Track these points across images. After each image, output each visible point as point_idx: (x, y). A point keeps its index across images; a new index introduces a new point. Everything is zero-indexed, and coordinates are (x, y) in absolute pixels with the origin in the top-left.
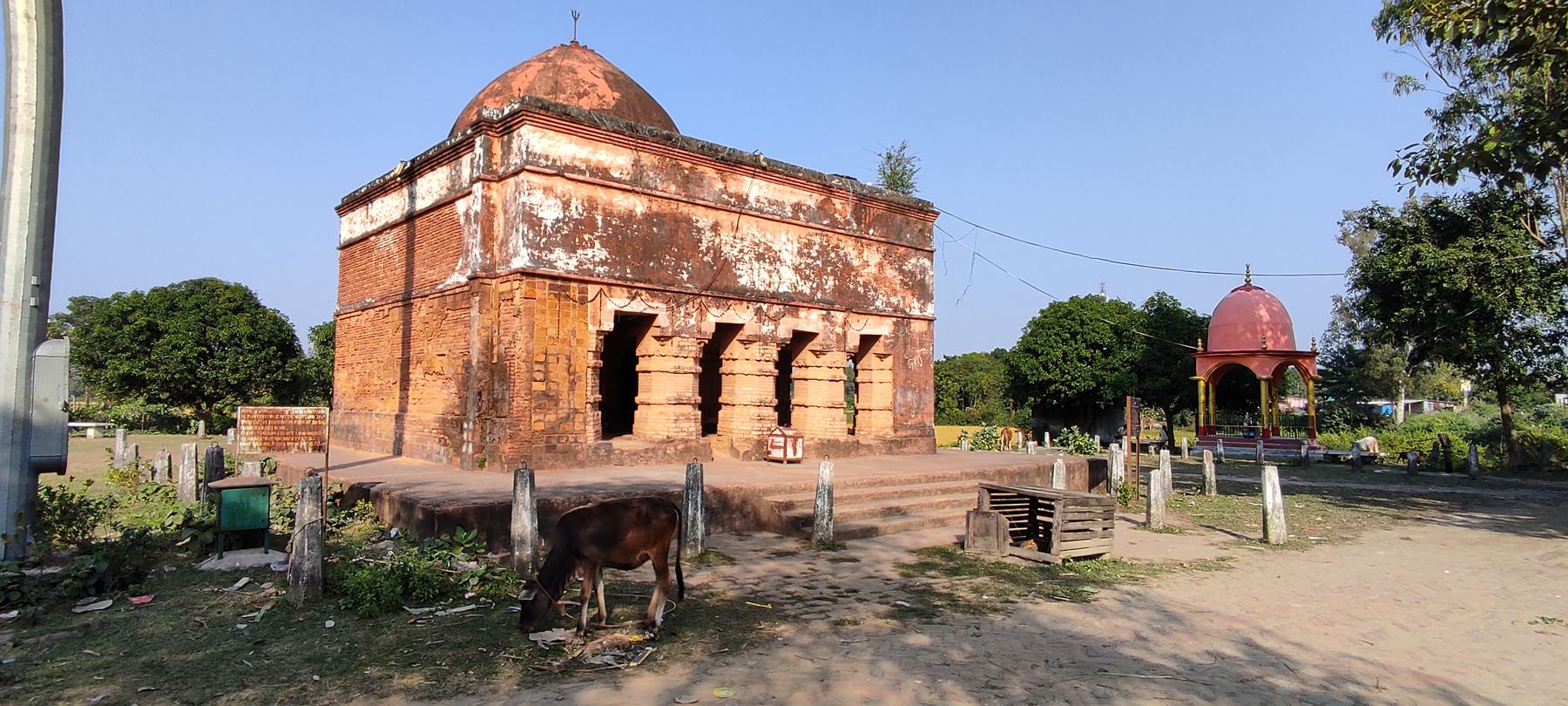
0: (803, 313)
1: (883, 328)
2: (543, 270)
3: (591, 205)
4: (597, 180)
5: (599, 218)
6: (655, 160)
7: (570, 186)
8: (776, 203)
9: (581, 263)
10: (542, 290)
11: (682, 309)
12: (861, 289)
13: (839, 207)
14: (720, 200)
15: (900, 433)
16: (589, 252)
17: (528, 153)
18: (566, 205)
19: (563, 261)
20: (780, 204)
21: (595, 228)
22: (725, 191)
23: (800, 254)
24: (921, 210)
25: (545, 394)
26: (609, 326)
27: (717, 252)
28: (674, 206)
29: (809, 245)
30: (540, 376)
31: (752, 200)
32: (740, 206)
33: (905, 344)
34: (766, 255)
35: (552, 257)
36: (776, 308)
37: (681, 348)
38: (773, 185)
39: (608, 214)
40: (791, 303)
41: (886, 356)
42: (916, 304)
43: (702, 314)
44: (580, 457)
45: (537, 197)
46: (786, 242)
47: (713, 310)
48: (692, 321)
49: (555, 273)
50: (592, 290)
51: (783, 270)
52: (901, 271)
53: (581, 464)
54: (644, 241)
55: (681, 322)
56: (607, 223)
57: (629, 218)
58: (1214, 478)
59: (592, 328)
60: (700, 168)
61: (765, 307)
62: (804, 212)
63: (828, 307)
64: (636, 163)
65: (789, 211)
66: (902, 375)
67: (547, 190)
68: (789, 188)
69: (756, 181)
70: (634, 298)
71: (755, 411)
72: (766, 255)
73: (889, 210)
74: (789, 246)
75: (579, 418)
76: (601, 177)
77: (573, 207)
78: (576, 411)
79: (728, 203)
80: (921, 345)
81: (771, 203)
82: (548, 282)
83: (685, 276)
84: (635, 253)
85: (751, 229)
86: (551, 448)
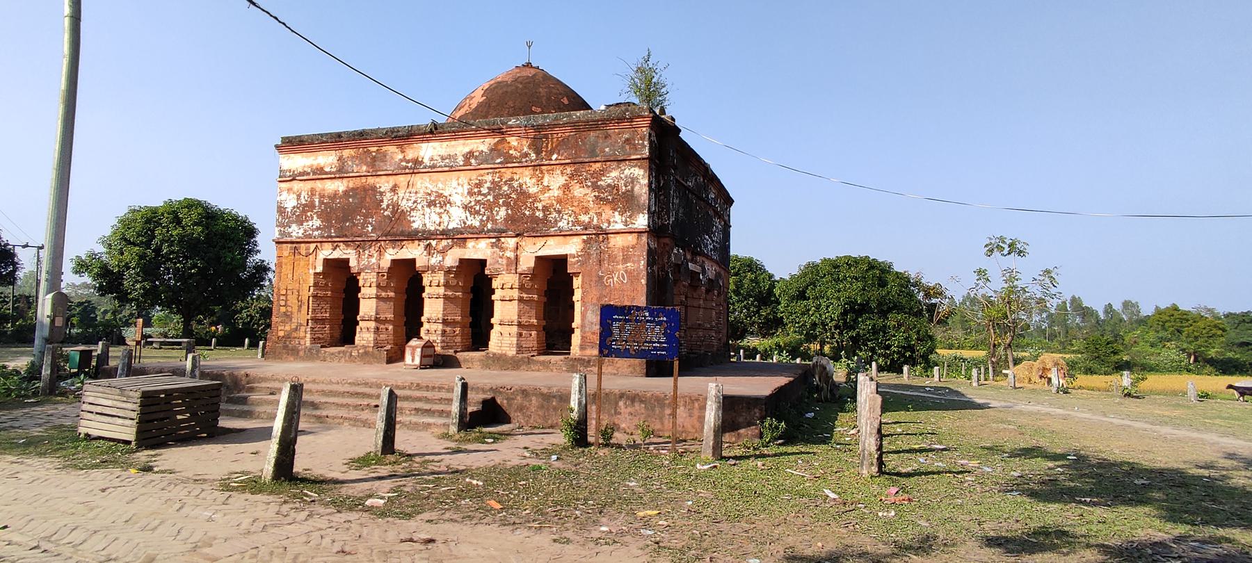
0: (470, 244)
1: (570, 248)
3: (313, 192)
6: (352, 152)
7: (302, 184)
12: (540, 214)
18: (299, 196)
19: (296, 231)
21: (314, 207)
22: (404, 160)
23: (470, 193)
24: (621, 119)
26: (320, 269)
27: (395, 207)
28: (364, 180)
29: (479, 185)
30: (283, 303)
31: (427, 161)
32: (416, 167)
33: (600, 262)
36: (444, 243)
39: (322, 196)
40: (458, 237)
43: (380, 252)
44: (301, 353)
45: (285, 195)
46: (457, 188)
47: (391, 251)
48: (374, 260)
50: (313, 246)
52: (595, 187)
55: (364, 262)
56: (321, 203)
57: (334, 196)
59: (312, 271)
60: (384, 148)
61: (434, 243)
62: (476, 158)
63: (498, 235)
65: (460, 161)
67: (289, 190)
68: (461, 141)
69: (431, 144)
70: (334, 249)
72: (438, 201)
73: (578, 130)
74: (460, 190)
75: (303, 329)
78: (301, 325)
81: (443, 159)
83: (370, 229)
84: (338, 220)
85: (423, 184)
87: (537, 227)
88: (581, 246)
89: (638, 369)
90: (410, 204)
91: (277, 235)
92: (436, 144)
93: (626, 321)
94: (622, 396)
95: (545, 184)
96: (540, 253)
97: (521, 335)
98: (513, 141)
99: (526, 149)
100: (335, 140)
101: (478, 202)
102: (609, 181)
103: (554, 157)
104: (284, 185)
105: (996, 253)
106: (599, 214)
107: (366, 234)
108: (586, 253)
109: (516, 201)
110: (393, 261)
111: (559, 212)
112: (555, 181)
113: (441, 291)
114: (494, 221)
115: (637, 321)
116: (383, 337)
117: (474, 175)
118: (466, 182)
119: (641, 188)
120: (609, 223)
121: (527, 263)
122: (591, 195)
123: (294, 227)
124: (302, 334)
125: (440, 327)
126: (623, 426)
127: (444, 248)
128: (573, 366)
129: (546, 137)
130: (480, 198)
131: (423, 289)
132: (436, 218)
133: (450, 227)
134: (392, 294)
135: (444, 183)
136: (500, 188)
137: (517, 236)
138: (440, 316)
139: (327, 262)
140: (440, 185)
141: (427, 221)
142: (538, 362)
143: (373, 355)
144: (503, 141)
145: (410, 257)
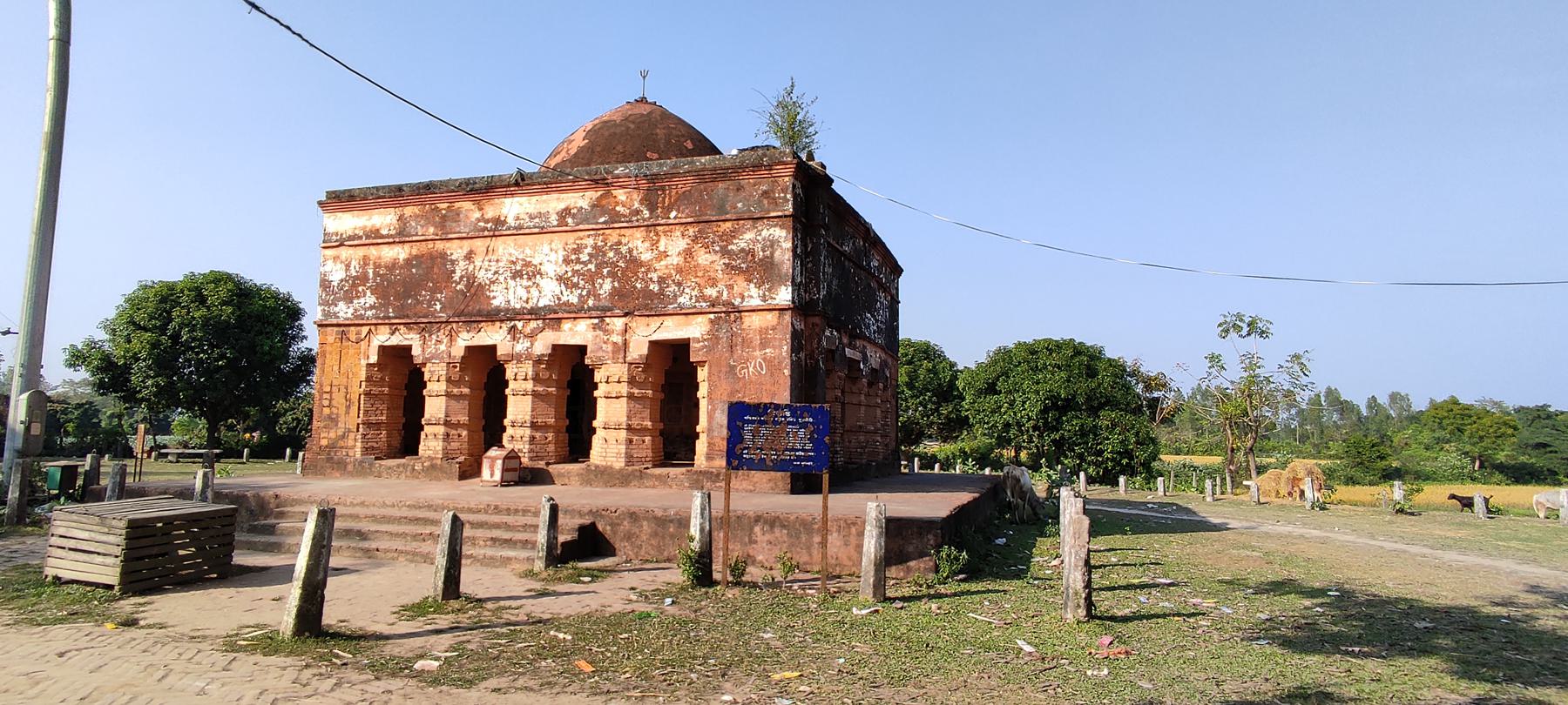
0: (566, 325)
1: (693, 329)
3: (365, 261)
6: (416, 210)
7: (351, 251)
12: (654, 287)
16: (362, 300)
18: (348, 266)
19: (344, 311)
22: (482, 219)
23: (567, 261)
24: (757, 166)
26: (374, 359)
27: (470, 279)
28: (430, 244)
29: (577, 250)
31: (511, 221)
32: (498, 228)
36: (533, 324)
38: (534, 199)
39: (377, 266)
40: (551, 317)
42: (754, 291)
44: (350, 467)
45: (330, 265)
47: (464, 335)
48: (443, 347)
49: (335, 321)
50: (365, 330)
51: (544, 283)
52: (725, 252)
54: (404, 283)
55: (431, 350)
56: (376, 274)
57: (393, 265)
59: (364, 362)
60: (457, 205)
61: (519, 325)
62: (574, 216)
63: (601, 314)
64: (400, 218)
65: (554, 219)
67: (336, 258)
68: (555, 196)
72: (526, 272)
73: (703, 180)
74: (553, 257)
75: (352, 436)
76: (374, 237)
80: (763, 345)
81: (531, 218)
83: (438, 307)
84: (398, 297)
85: (507, 249)
87: (651, 304)
89: (781, 484)
90: (490, 275)
91: (319, 316)
92: (524, 199)
93: (761, 423)
94: (758, 519)
95: (662, 249)
96: (655, 337)
97: (630, 441)
98: (621, 195)
99: (637, 205)
100: (395, 195)
101: (575, 272)
102: (743, 245)
103: (673, 214)
104: (329, 252)
105: (1233, 335)
106: (730, 287)
107: (433, 314)
108: (713, 338)
109: (624, 271)
110: (468, 348)
111: (679, 284)
112: (674, 245)
113: (529, 385)
114: (597, 297)
115: (775, 423)
116: (455, 445)
117: (571, 238)
118: (560, 246)
119: (783, 253)
120: (743, 298)
121: (639, 349)
122: (720, 262)
123: (342, 305)
124: (351, 443)
125: (528, 432)
126: (760, 558)
127: (533, 331)
128: (697, 481)
129: (663, 189)
130: (578, 267)
131: (506, 384)
132: (522, 293)
133: (541, 304)
134: (466, 391)
136: (605, 254)
137: (626, 315)
138: (528, 418)
139: (384, 350)
140: (528, 251)
141: (511, 297)
142: (653, 476)
143: (441, 469)
144: (608, 194)
145: (490, 342)
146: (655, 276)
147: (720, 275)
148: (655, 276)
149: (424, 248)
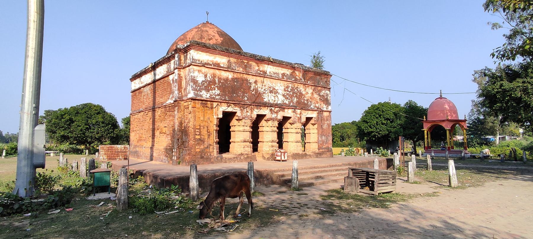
0: (286, 110)
1: (314, 115)
2: (198, 98)
3: (214, 76)
4: (216, 67)
5: (217, 80)
6: (235, 60)
7: (207, 70)
8: (276, 73)
9: (211, 95)
10: (198, 104)
11: (245, 110)
12: (306, 102)
13: (298, 74)
14: (257, 73)
15: (320, 151)
16: (214, 91)
17: (193, 59)
19: (205, 95)
20: (278, 74)
22: (259, 70)
23: (285, 90)
25: (200, 139)
26: (221, 116)
27: (256, 90)
28: (242, 75)
29: (288, 87)
30: (198, 133)
31: (268, 72)
32: (264, 75)
34: (273, 91)
35: (201, 93)
36: (277, 109)
37: (245, 123)
38: (275, 67)
39: (220, 79)
40: (282, 107)
41: (315, 124)
42: (325, 106)
46: (280, 86)
47: (256, 110)
48: (249, 114)
49: (202, 99)
50: (215, 104)
51: (279, 96)
52: (319, 95)
53: (212, 163)
55: (245, 114)
56: (219, 82)
57: (227, 80)
58: (431, 164)
59: (215, 117)
60: (250, 63)
61: (273, 108)
63: (294, 108)
64: (229, 61)
66: (321, 131)
69: (269, 66)
71: (270, 144)
72: (273, 91)
73: (315, 75)
74: (281, 88)
75: (211, 147)
76: (217, 66)
77: (208, 77)
78: (210, 145)
79: (260, 74)
80: (327, 120)
81: (274, 74)
82: (200, 102)
83: (246, 99)
84: (229, 91)
85: (268, 82)
86: (202, 157)
88: (317, 115)
90: (263, 90)
92: (271, 67)
98: (297, 73)
101: (287, 94)
109: (299, 96)
135: (275, 84)
144: (294, 72)
146: (306, 99)
147: (318, 101)
148: (306, 99)
149: (239, 76)
